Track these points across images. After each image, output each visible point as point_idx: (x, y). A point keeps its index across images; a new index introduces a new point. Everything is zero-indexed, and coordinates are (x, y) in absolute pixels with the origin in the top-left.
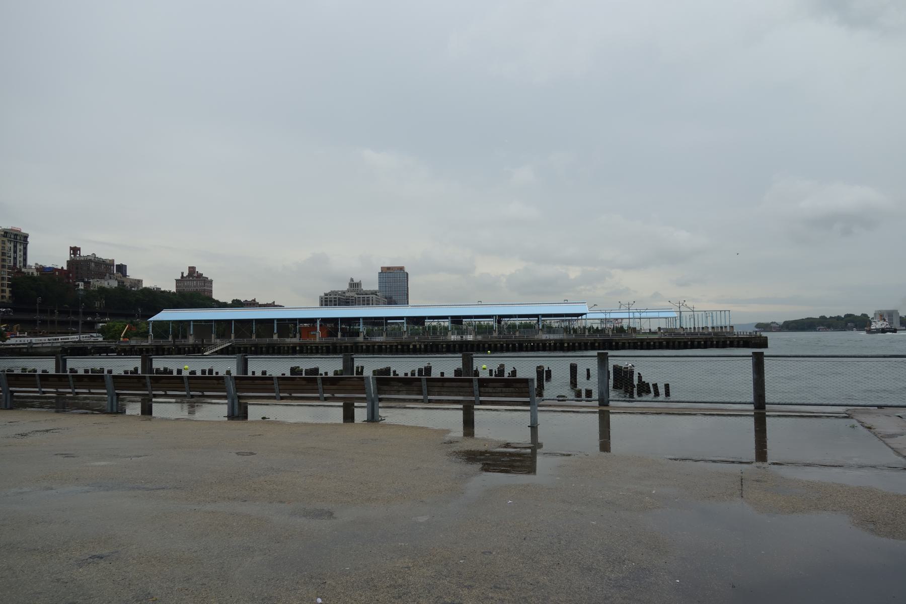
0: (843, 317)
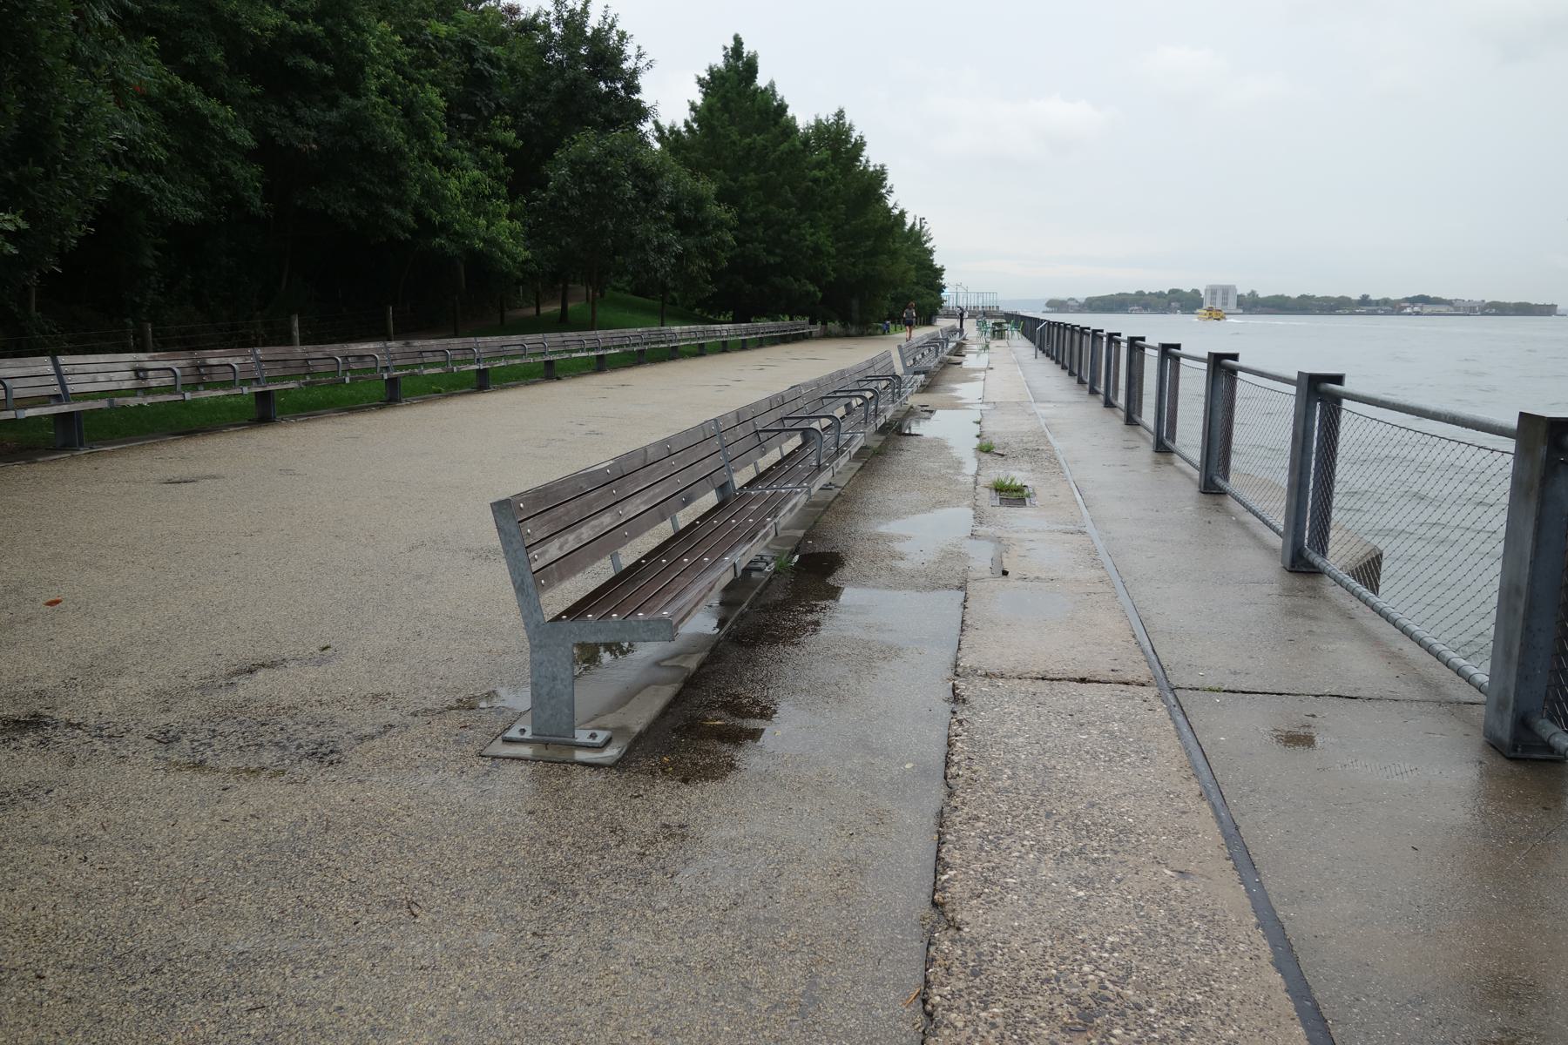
0: (1166, 292)
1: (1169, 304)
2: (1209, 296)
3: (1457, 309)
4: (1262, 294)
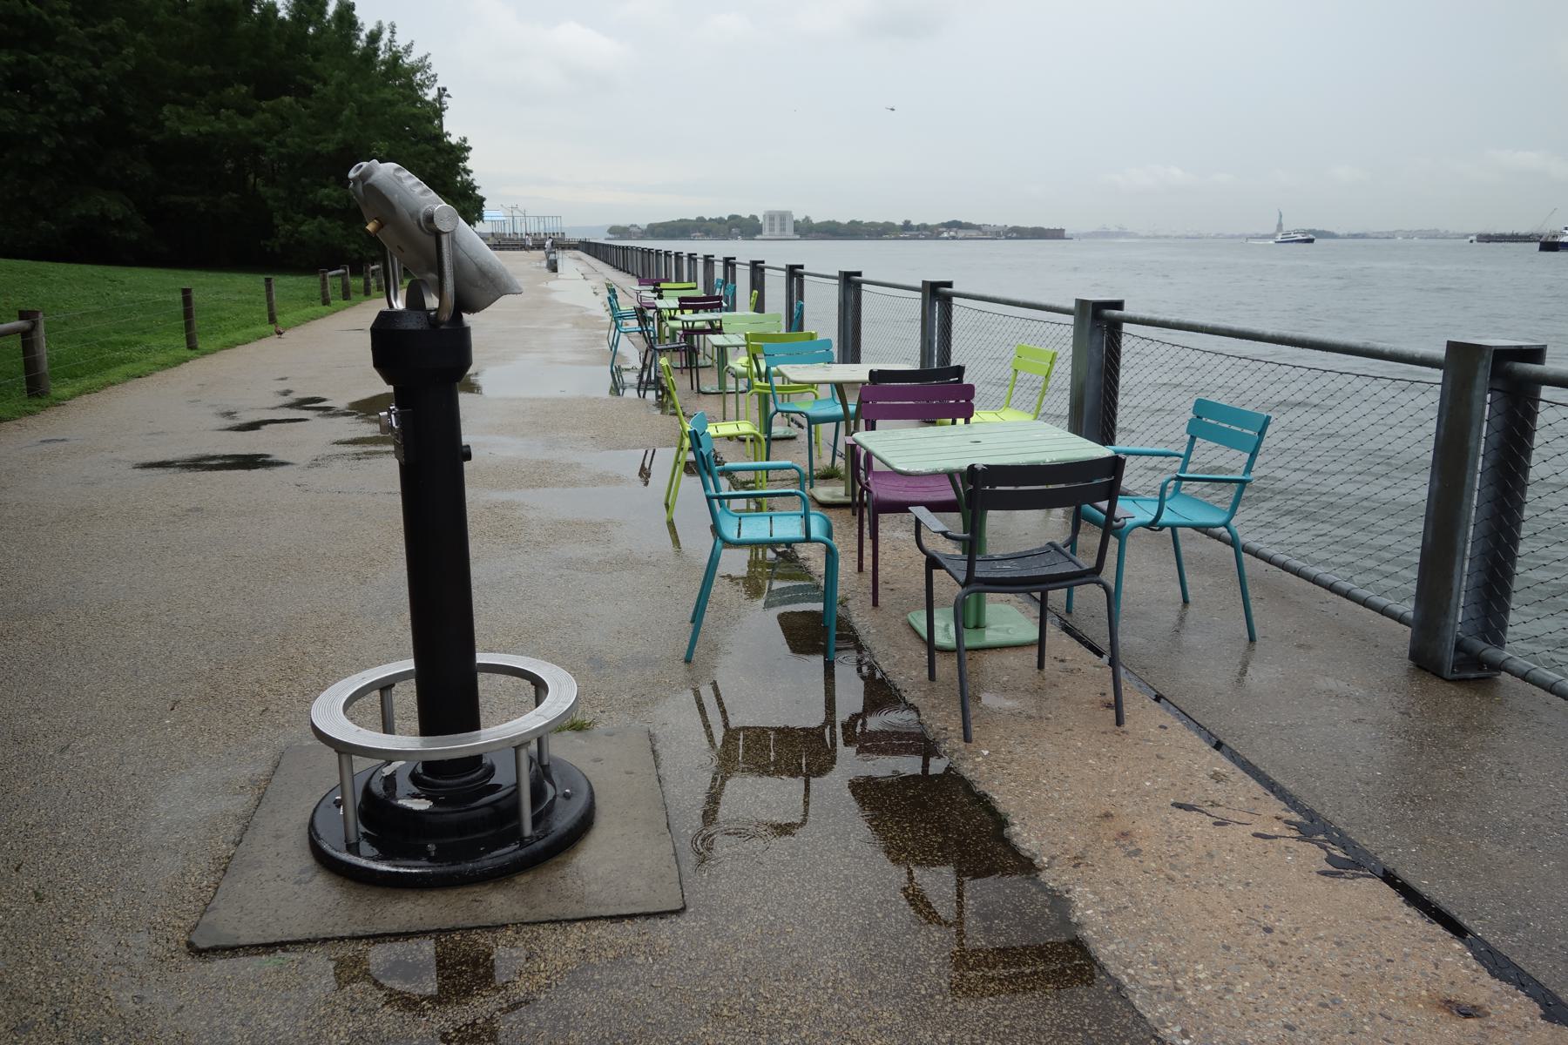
0: (726, 219)
1: (730, 230)
2: (767, 222)
3: (985, 233)
4: (816, 220)
